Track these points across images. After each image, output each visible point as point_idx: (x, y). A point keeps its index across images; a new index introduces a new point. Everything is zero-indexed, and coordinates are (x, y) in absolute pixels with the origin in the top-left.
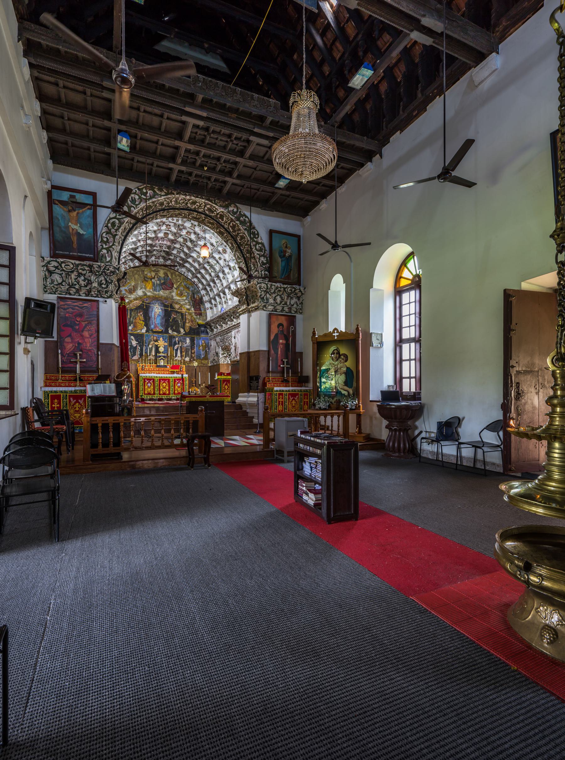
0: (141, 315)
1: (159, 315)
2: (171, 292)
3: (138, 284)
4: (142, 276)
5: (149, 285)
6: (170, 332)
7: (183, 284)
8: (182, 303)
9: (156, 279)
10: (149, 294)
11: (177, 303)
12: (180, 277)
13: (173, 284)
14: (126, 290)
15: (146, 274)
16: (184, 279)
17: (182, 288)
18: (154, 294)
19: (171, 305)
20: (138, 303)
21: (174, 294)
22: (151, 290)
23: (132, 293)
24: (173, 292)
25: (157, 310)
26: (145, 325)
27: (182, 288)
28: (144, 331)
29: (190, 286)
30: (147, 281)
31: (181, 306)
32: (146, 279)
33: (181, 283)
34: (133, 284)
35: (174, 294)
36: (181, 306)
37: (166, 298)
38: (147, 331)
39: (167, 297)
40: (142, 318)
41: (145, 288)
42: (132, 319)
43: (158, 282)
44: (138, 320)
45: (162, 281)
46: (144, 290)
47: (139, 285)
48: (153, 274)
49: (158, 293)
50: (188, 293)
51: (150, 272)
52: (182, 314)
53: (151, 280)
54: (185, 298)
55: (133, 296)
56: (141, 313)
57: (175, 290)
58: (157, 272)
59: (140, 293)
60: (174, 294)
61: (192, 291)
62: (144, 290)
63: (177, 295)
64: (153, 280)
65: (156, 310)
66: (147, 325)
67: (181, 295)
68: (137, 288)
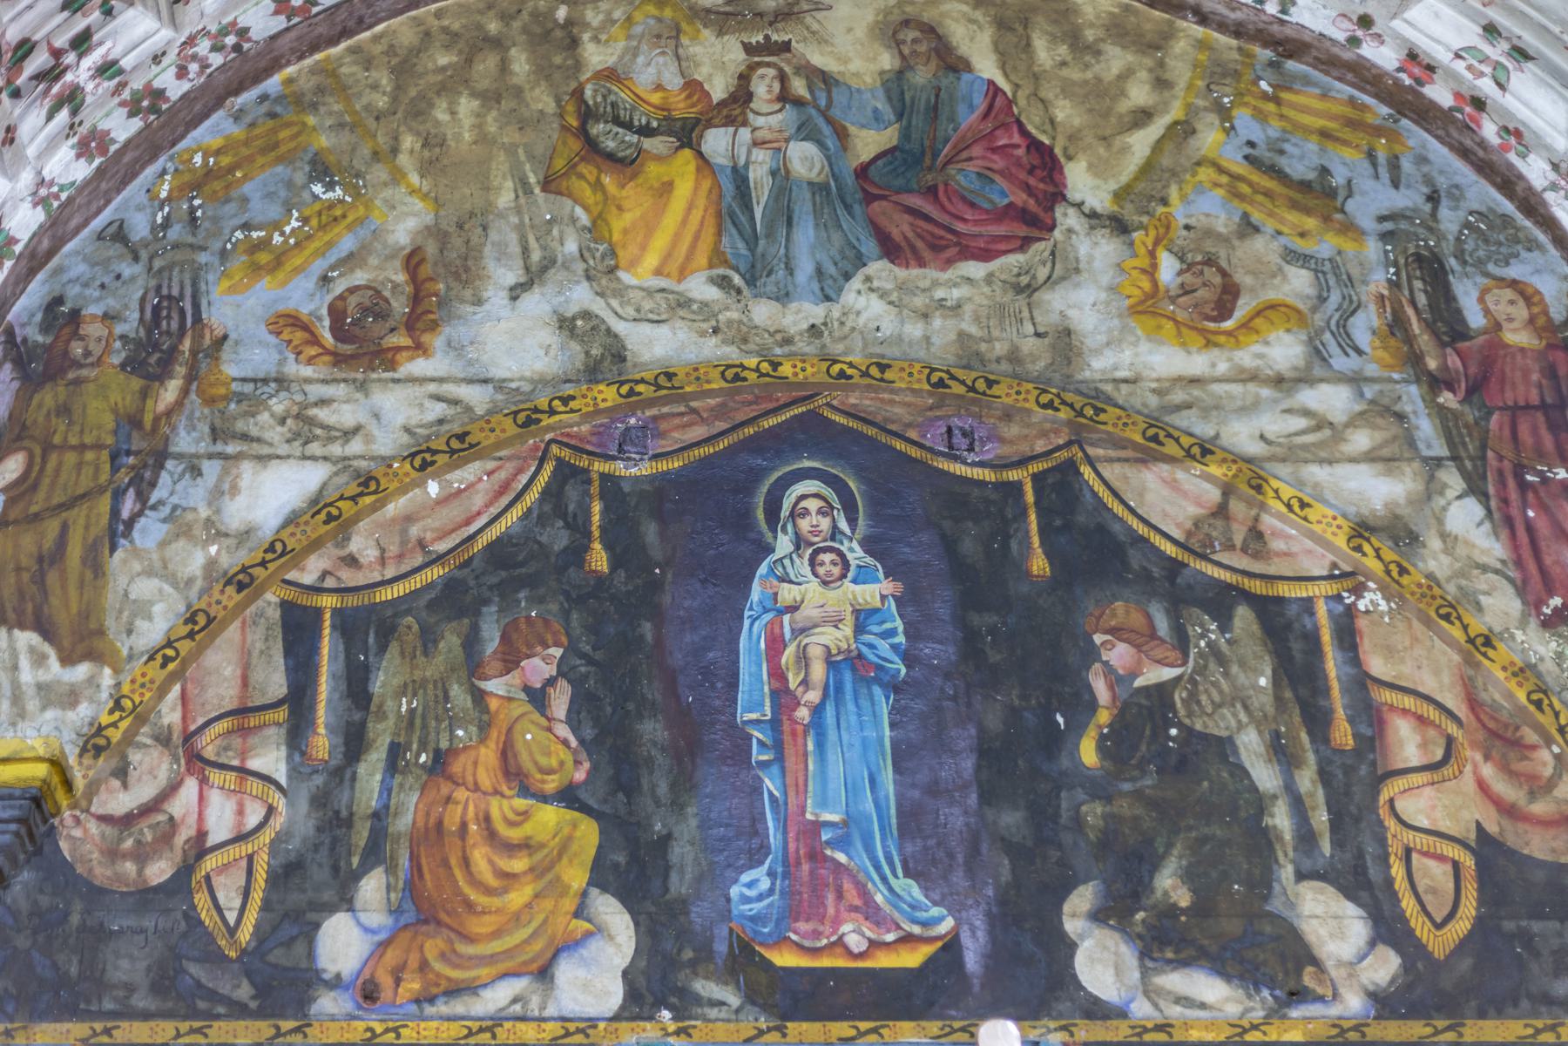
0: (528, 706)
1: (851, 667)
2: (1026, 289)
3: (477, 219)
6: (1102, 963)
7: (1209, 138)
8: (1241, 435)
10: (656, 344)
11: (1157, 441)
12: (1154, 45)
14: (287, 323)
16: (1217, 73)
17: (1204, 207)
19: (1060, 486)
20: (472, 503)
21: (1083, 306)
22: (700, 288)
23: (385, 359)
24: (1066, 270)
25: (820, 597)
26: (602, 876)
28: (593, 982)
29: (1345, 164)
30: (626, 164)
31: (1251, 477)
33: (1183, 131)
35: (1091, 303)
36: (1251, 477)
37: (963, 387)
38: (652, 988)
39: (969, 353)
40: (554, 747)
41: (603, 267)
42: (371, 773)
44: (477, 794)
46: (581, 296)
47: (504, 233)
49: (816, 312)
50: (1328, 272)
52: (1282, 627)
54: (1283, 350)
55: (391, 412)
56: (538, 668)
59: (510, 339)
60: (1091, 303)
61: (1393, 228)
62: (581, 296)
63: (1147, 306)
65: (808, 593)
66: (633, 869)
67: (1213, 303)
68: (466, 273)
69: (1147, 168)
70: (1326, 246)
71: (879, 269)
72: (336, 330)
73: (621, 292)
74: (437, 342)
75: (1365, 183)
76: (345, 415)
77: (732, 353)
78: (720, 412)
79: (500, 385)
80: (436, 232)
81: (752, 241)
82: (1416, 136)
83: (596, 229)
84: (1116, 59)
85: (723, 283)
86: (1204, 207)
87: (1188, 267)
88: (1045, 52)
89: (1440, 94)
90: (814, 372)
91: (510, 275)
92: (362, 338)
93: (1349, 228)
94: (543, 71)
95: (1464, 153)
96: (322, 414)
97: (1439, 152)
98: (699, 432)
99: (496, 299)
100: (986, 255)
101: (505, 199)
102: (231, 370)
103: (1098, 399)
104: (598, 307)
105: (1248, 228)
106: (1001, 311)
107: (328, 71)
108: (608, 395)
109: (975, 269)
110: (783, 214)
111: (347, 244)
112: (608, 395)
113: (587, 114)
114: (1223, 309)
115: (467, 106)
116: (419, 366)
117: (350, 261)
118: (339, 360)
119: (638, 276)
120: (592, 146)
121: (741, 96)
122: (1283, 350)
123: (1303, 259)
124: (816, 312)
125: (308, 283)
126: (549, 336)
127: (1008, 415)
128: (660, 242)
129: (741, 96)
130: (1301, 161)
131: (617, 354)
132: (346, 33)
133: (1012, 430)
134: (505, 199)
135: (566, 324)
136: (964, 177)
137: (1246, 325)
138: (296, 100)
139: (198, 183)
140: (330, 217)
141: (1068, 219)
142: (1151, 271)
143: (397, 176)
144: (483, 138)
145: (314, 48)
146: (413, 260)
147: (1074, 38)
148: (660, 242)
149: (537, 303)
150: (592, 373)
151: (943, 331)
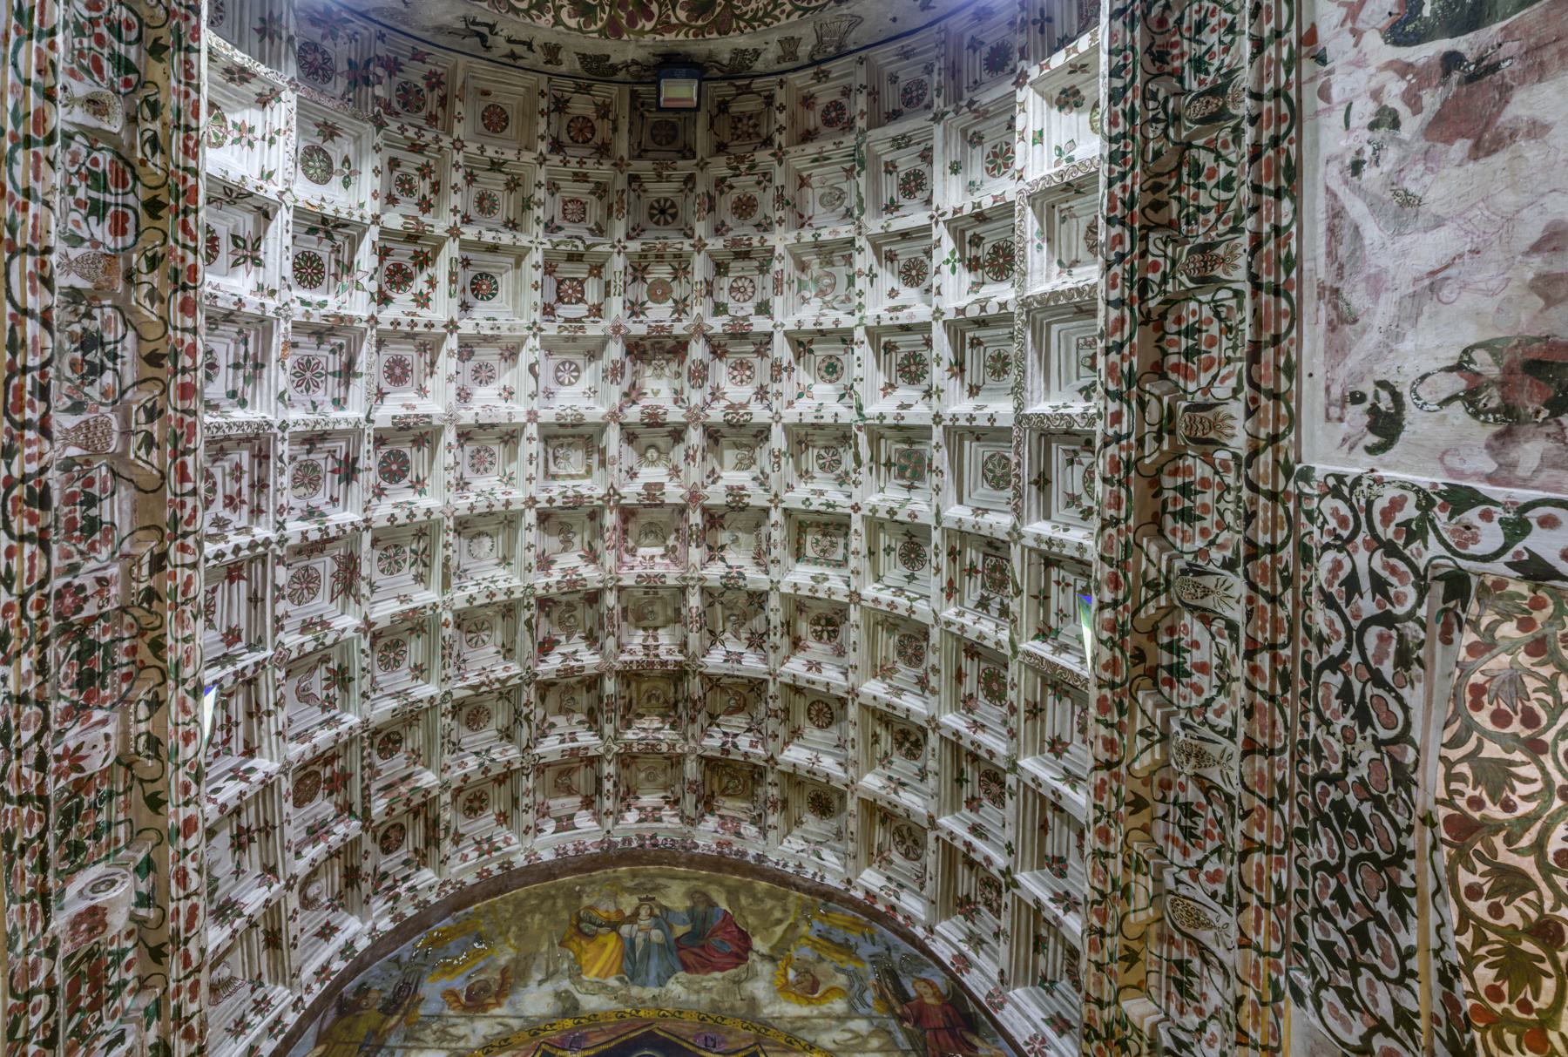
2: (738, 982)
3: (533, 956)
4: (565, 915)
5: (602, 957)
7: (804, 929)
9: (645, 921)
10: (591, 1002)
13: (744, 939)
14: (451, 994)
15: (591, 907)
16: (805, 907)
18: (626, 1000)
21: (759, 989)
22: (612, 982)
24: (753, 975)
27: (804, 953)
29: (854, 937)
30: (591, 937)
32: (583, 928)
34: (503, 960)
39: (715, 1007)
41: (576, 974)
43: (656, 935)
45: (680, 930)
46: (565, 984)
48: (628, 903)
49: (656, 991)
51: (614, 896)
53: (614, 927)
57: (765, 968)
58: (648, 893)
59: (536, 1000)
61: (875, 959)
62: (565, 984)
63: (784, 989)
64: (625, 929)
67: (808, 987)
69: (782, 939)
70: (851, 965)
71: (682, 975)
72: (468, 997)
73: (581, 983)
74: (506, 1002)
75: (862, 944)
76: (461, 1031)
77: (621, 1007)
78: (612, 1031)
79: (526, 1019)
80: (516, 961)
81: (634, 964)
82: (879, 928)
83: (576, 960)
84: (769, 903)
85: (621, 980)
86: (804, 953)
87: (799, 974)
88: (744, 901)
89: (881, 907)
90: (653, 1014)
91: (539, 977)
92: (476, 1001)
93: (858, 959)
94: (567, 907)
95: (896, 932)
96: (452, 1030)
97: (888, 933)
98: (603, 1039)
99: (533, 985)
100: (722, 969)
101: (544, 949)
102: (421, 1012)
103: (766, 1025)
104: (571, 988)
105: (821, 959)
106: (728, 991)
107: (491, 905)
108: (569, 1023)
109: (718, 975)
110: (647, 954)
111: (481, 964)
112: (569, 1023)
113: (580, 920)
114: (814, 991)
115: (538, 917)
116: (497, 1011)
117: (481, 971)
118: (465, 1008)
119: (589, 977)
120: (580, 931)
121: (636, 914)
122: (839, 1006)
123: (843, 971)
124: (656, 991)
125: (462, 978)
126: (551, 1000)
127: (730, 1032)
128: (599, 965)
129: (636, 914)
130: (838, 936)
131: (576, 1006)
132: (500, 892)
133: (732, 1039)
134: (544, 949)
135: (558, 995)
136: (714, 942)
137: (823, 996)
138: (478, 914)
139: (433, 942)
140: (478, 954)
141: (753, 957)
142: (785, 975)
143: (506, 940)
144: (542, 928)
145: (488, 896)
146: (504, 971)
147: (754, 896)
148: (599, 965)
149: (548, 987)
150: (564, 1014)
151: (705, 998)
